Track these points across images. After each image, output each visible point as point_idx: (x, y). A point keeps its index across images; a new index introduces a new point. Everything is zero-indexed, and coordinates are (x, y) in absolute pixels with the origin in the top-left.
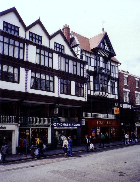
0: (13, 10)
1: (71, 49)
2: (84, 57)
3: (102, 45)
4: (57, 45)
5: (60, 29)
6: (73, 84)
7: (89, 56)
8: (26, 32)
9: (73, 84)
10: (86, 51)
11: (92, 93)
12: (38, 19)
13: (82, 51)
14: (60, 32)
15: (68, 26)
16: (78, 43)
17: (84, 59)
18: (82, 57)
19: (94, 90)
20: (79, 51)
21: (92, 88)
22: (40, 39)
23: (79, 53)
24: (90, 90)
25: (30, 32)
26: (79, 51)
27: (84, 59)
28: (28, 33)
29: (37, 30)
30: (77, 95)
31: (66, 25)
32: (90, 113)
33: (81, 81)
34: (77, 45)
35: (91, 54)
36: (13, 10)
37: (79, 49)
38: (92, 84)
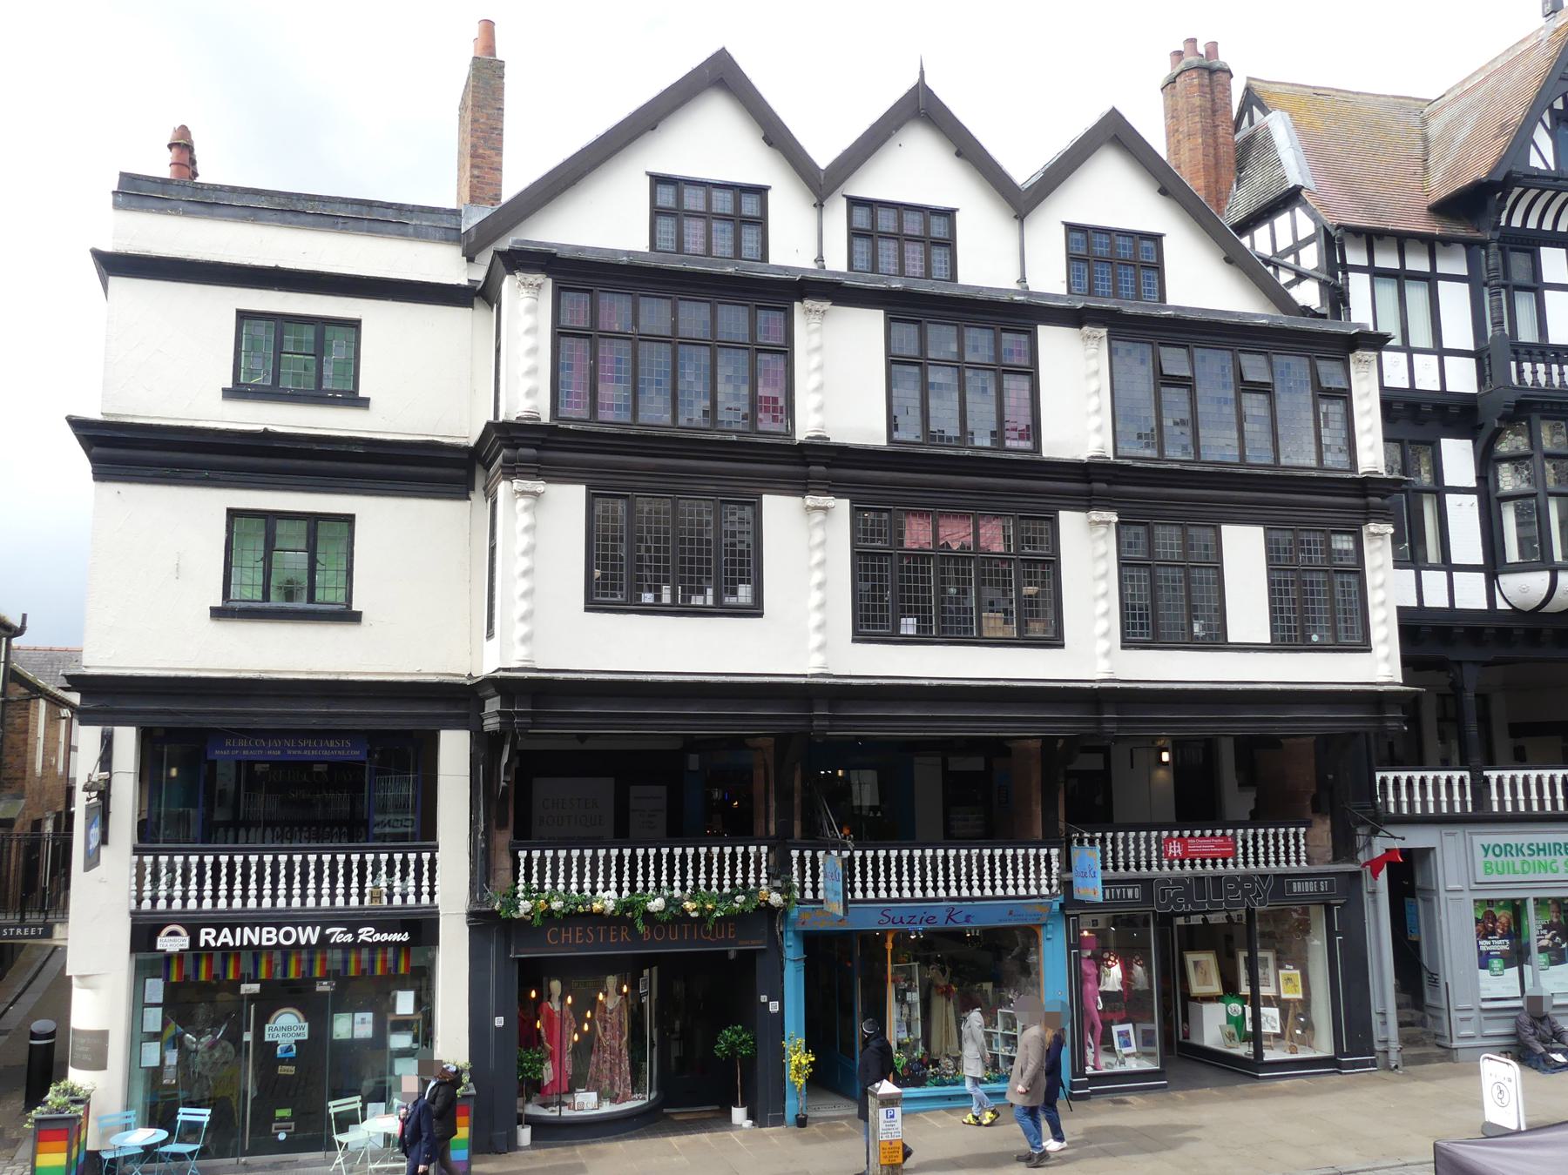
0: (720, 77)
1: (1228, 242)
2: (1359, 286)
3: (1543, 139)
4: (1089, 247)
5: (1107, 109)
6: (1244, 551)
7: (1418, 263)
8: (819, 206)
9: (1244, 551)
10: (1371, 238)
11: (1471, 594)
12: (913, 80)
13: (1333, 241)
14: (1114, 133)
15: (1213, 48)
16: (1294, 170)
17: (1360, 313)
18: (1337, 298)
19: (1494, 565)
20: (1308, 241)
21: (1467, 543)
22: (935, 230)
23: (1310, 258)
24: (1447, 565)
25: (854, 202)
26: (1308, 241)
27: (1360, 313)
28: (837, 219)
29: (915, 173)
30: (1290, 633)
31: (1192, 41)
32: (1456, 775)
33: (1315, 514)
34: (1290, 199)
35: (1431, 244)
36: (720, 77)
37: (1306, 227)
38: (1464, 516)
